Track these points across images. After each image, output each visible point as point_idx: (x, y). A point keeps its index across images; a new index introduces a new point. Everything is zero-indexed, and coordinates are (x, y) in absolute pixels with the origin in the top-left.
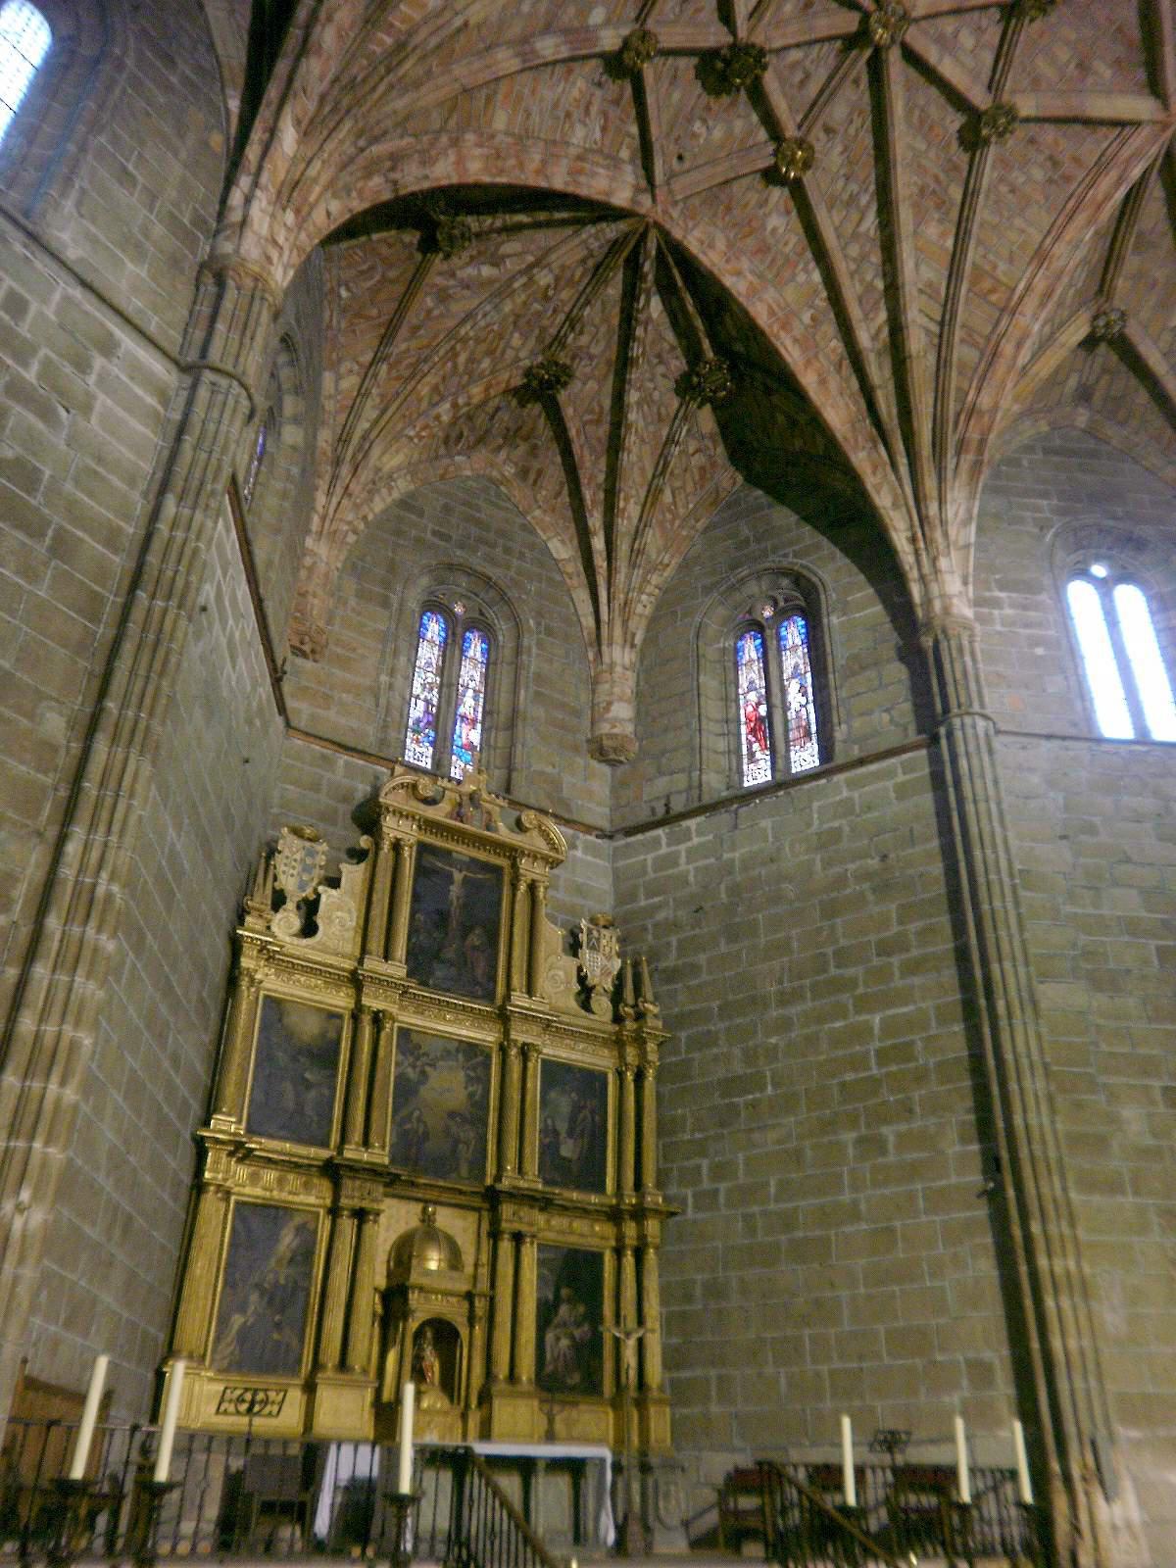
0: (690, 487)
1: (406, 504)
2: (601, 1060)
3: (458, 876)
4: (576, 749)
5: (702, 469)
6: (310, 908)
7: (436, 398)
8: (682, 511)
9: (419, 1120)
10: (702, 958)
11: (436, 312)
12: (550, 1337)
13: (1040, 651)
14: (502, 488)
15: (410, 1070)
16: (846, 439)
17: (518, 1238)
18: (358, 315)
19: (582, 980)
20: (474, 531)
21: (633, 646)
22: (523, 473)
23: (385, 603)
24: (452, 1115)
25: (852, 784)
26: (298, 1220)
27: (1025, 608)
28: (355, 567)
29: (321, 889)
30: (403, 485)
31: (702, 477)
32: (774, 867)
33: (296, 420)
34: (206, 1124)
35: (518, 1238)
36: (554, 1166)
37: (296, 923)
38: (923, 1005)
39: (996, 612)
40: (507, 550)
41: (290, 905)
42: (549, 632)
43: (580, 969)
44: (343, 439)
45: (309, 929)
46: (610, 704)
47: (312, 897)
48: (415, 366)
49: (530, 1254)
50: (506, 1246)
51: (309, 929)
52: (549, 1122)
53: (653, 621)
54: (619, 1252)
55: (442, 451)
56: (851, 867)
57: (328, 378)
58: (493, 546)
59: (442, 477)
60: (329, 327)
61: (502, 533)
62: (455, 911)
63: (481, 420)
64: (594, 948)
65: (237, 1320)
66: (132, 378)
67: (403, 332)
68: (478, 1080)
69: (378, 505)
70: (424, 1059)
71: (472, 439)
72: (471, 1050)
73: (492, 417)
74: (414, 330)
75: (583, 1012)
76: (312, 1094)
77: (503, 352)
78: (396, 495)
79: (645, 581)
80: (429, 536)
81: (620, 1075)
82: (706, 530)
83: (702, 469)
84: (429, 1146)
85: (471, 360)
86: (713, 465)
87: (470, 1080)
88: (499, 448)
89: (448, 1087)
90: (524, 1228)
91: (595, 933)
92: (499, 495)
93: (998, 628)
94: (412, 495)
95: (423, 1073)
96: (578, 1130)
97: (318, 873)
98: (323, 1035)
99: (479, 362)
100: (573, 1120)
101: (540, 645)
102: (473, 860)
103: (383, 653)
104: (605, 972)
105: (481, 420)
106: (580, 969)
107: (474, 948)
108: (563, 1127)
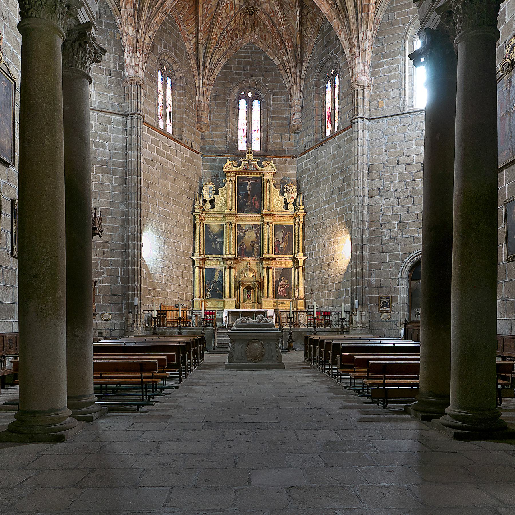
0: (310, 27)
1: (225, 68)
2: (291, 222)
3: (249, 183)
4: (287, 132)
5: (312, 18)
6: (212, 201)
7: (222, 31)
8: (309, 36)
9: (244, 245)
10: (311, 193)
11: (209, 8)
12: (279, 288)
13: (393, 81)
14: (256, 45)
15: (241, 234)
16: (329, 17)
17: (268, 268)
18: (188, 20)
19: (285, 202)
20: (248, 66)
21: (301, 91)
22: (261, 37)
23: (224, 105)
24: (252, 242)
25: (339, 139)
26: (219, 270)
27: (392, 64)
28: (214, 97)
29: (214, 196)
30: (223, 61)
31: (312, 21)
32: (324, 165)
33: (178, 70)
34: (193, 255)
35: (268, 268)
36: (278, 250)
37: (210, 206)
38: (346, 206)
39: (381, 69)
40: (260, 69)
41: (208, 202)
42: (276, 94)
43: (285, 199)
44: (198, 60)
45: (213, 207)
46: (294, 114)
47: (213, 199)
48: (210, 26)
49: (271, 271)
50: (265, 270)
51: (213, 207)
52: (277, 240)
53: (305, 80)
54: (295, 268)
55: (233, 42)
56: (337, 165)
57: (187, 44)
58: (255, 70)
59: (236, 51)
60: (181, 29)
61: (258, 64)
62: (249, 192)
63: (241, 27)
64: (288, 192)
65: (209, 290)
66: (116, 125)
67: (201, 19)
68: (258, 232)
69: (217, 72)
70: (244, 231)
71: (241, 34)
72: (255, 226)
73: (244, 24)
74: (205, 16)
75: (286, 211)
76: (219, 244)
77: (235, 7)
78: (222, 65)
79: (302, 65)
80: (235, 76)
81: (295, 224)
82: (317, 41)
83: (312, 18)
84: (247, 250)
85: (226, 15)
86: (315, 15)
87: (256, 233)
88: (252, 31)
89: (251, 236)
90: (268, 266)
91: (289, 188)
92: (256, 48)
93: (380, 75)
94: (227, 63)
95: (245, 234)
96: (285, 240)
97: (213, 193)
98: (220, 230)
99: (230, 13)
100: (283, 238)
101: (273, 100)
102: (254, 177)
103: (226, 122)
104: (292, 198)
105: (241, 27)
106: (285, 199)
107: (255, 200)
108: (280, 240)
